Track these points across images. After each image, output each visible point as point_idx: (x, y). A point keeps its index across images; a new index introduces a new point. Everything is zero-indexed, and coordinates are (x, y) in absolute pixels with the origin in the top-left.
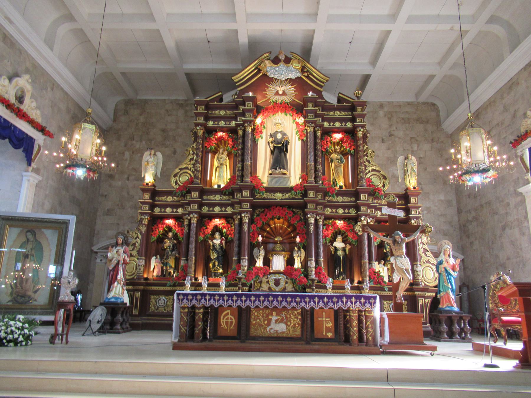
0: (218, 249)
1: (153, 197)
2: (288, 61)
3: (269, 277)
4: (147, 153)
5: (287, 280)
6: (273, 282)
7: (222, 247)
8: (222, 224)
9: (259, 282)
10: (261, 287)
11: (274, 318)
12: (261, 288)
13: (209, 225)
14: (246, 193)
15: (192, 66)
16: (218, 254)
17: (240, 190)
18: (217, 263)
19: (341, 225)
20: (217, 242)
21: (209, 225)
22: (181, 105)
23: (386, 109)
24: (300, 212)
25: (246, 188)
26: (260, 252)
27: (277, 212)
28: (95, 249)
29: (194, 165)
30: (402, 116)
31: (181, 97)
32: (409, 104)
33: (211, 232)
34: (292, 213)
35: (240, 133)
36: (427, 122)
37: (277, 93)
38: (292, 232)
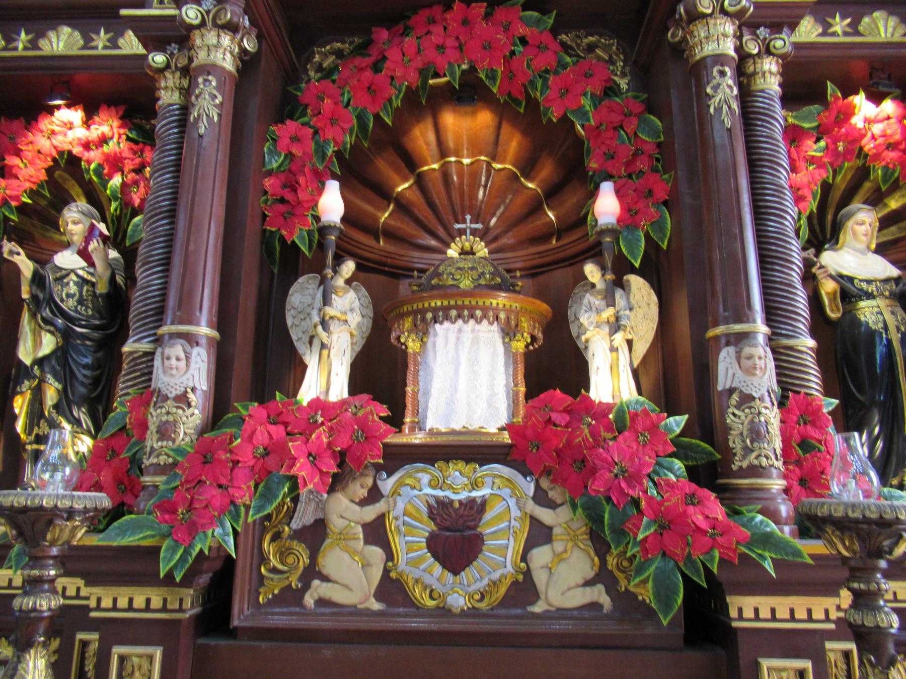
0: (69, 305)
3: (387, 484)
5: (546, 515)
6: (427, 527)
8: (104, 140)
9: (298, 535)
10: (312, 573)
12: (319, 589)
13: (18, 153)
16: (66, 335)
18: (51, 395)
19: (877, 129)
21: (18, 153)
26: (326, 301)
27: (451, 42)
33: (32, 194)
34: (558, 48)
38: (552, 193)
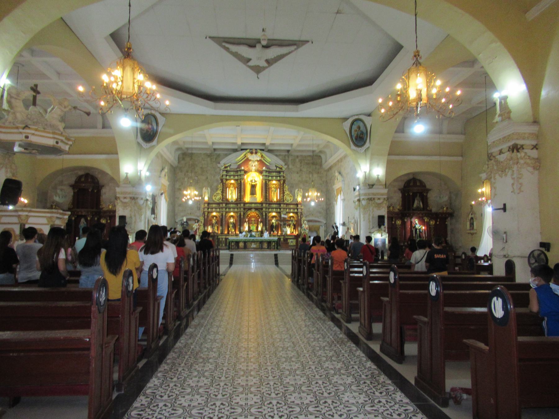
1: (208, 205)
2: (256, 153)
4: (204, 189)
7: (233, 223)
11: (253, 244)
14: (242, 205)
15: (216, 147)
17: (240, 203)
20: (232, 220)
22: (209, 156)
23: (299, 158)
24: (261, 210)
25: (242, 203)
28: (177, 221)
29: (222, 192)
30: (306, 161)
31: (209, 152)
32: (310, 156)
35: (239, 182)
36: (317, 164)
37: (252, 166)
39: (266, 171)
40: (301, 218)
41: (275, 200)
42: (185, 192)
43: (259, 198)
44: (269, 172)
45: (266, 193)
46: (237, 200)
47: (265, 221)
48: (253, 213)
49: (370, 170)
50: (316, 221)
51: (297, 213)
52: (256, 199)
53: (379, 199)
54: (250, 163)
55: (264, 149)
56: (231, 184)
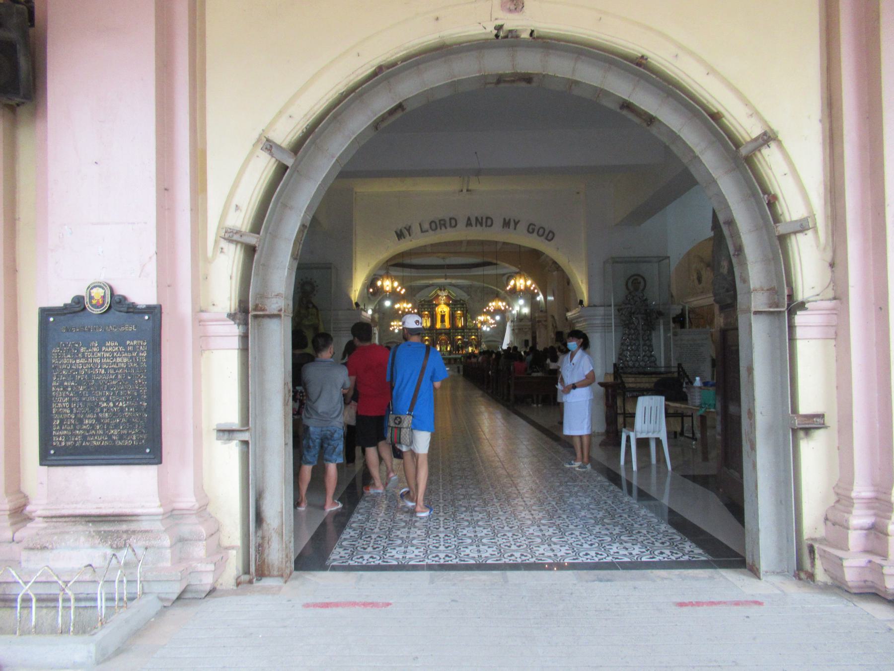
2: (444, 290)
39: (452, 304)
40: (481, 339)
41: (460, 326)
42: (392, 324)
43: (447, 324)
44: (455, 305)
45: (453, 321)
46: (430, 327)
47: (453, 343)
48: (443, 337)
49: (520, 309)
50: (494, 341)
51: (477, 336)
52: (445, 326)
53: (526, 329)
54: (440, 297)
55: (451, 285)
56: (426, 314)
